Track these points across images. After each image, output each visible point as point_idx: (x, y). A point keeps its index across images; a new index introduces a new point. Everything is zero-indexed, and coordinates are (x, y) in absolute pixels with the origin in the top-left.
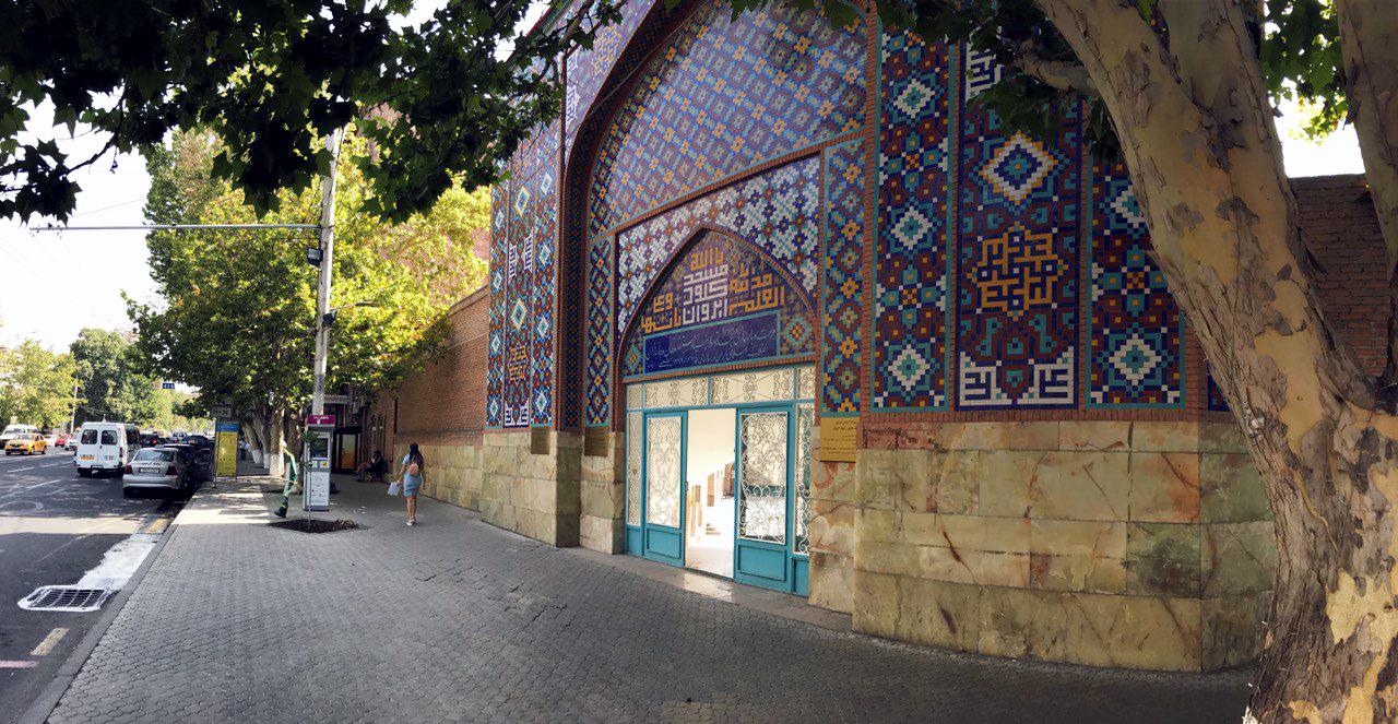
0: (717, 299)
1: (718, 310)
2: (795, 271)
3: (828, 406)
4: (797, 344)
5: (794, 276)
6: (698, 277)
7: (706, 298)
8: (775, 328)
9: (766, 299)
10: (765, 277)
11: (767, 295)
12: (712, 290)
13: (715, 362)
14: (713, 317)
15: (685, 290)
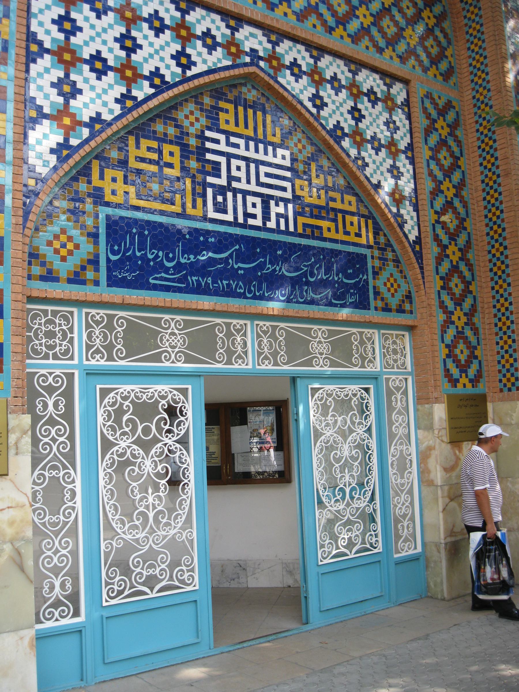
1: (278, 215)
4: (394, 303)
6: (237, 146)
7: (253, 187)
12: (263, 179)
14: (271, 224)
15: (209, 156)
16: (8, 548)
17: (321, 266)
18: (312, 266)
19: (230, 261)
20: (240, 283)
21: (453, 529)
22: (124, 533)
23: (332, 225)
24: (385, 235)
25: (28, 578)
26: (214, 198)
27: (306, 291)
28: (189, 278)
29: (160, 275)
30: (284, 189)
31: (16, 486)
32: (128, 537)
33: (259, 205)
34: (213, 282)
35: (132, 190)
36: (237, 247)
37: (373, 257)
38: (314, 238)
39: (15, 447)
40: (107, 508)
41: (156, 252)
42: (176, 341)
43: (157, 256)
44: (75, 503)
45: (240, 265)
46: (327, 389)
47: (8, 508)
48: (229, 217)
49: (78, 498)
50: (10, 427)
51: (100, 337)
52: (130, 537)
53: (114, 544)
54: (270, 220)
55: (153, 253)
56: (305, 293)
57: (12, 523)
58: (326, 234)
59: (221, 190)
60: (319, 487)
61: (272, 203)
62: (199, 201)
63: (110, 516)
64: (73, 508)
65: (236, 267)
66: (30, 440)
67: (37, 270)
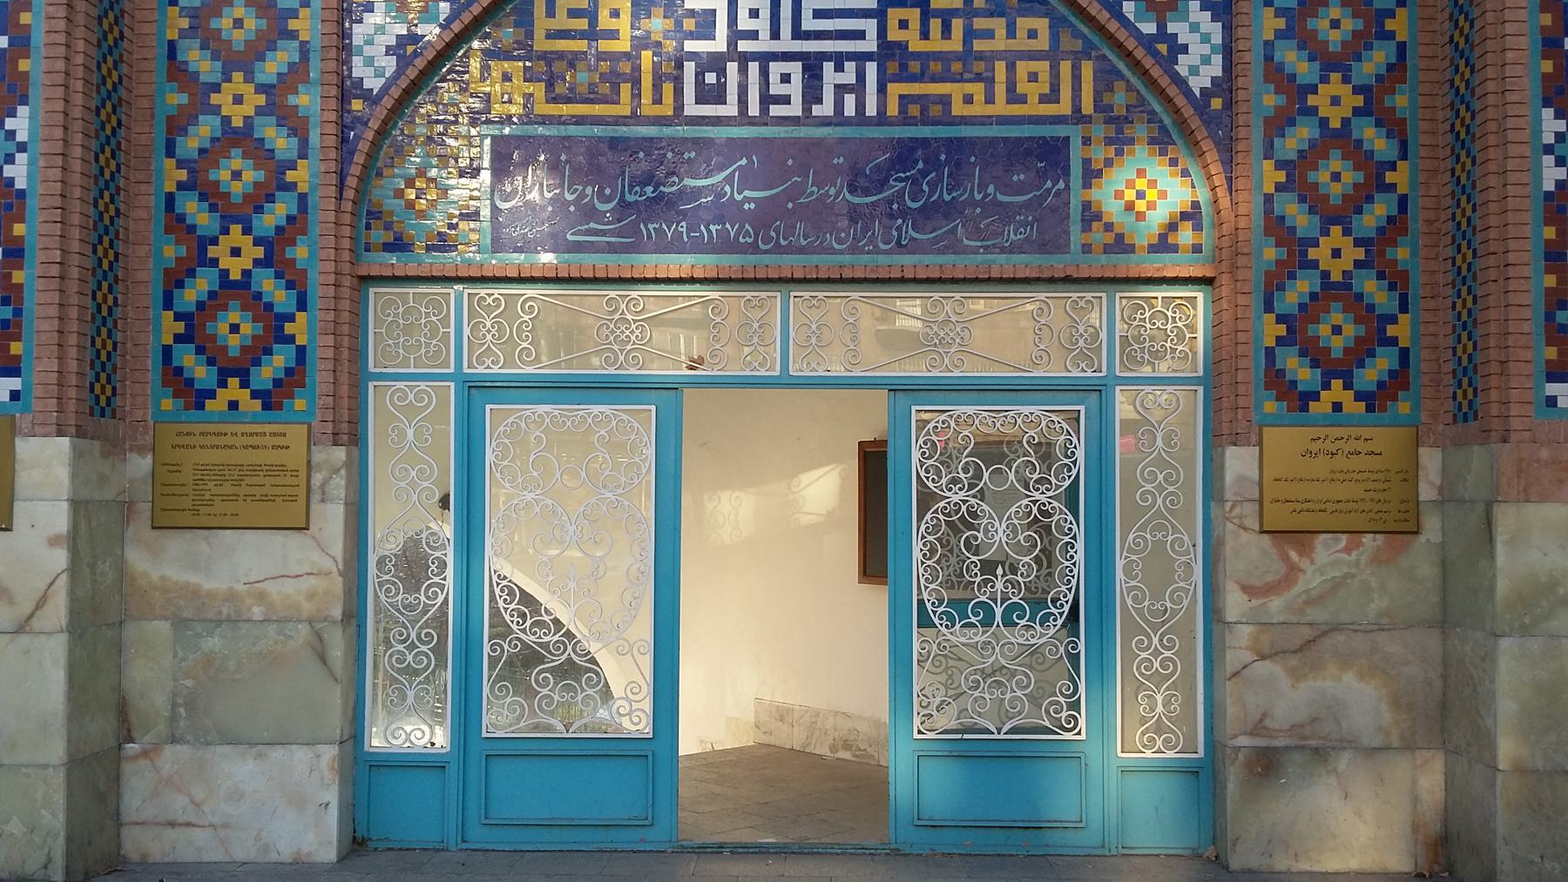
0: (839, 60)
1: (841, 89)
2: (1149, 28)
3: (1395, 398)
5: (1148, 42)
7: (787, 44)
8: (1066, 172)
9: (1032, 91)
10: (1024, 24)
11: (1033, 77)
12: (808, 24)
13: (831, 251)
14: (826, 109)
16: (304, 629)
17: (940, 179)
18: (915, 182)
19: (727, 189)
20: (747, 226)
21: (1261, 721)
22: (524, 631)
23: (977, 89)
24: (1130, 88)
25: (331, 673)
26: (700, 75)
27: (899, 229)
28: (642, 226)
29: (586, 227)
30: (860, 35)
31: (319, 545)
32: (530, 639)
33: (797, 79)
34: (689, 231)
35: (538, 90)
36: (744, 162)
37: (1087, 141)
38: (925, 120)
39: (320, 491)
40: (497, 591)
41: (581, 188)
42: (627, 332)
43: (583, 195)
44: (444, 579)
45: (747, 193)
46: (957, 413)
47: (307, 574)
48: (730, 109)
49: (450, 572)
50: (313, 464)
51: (494, 331)
52: (533, 638)
53: (506, 647)
54: (819, 101)
55: (577, 190)
56: (895, 233)
57: (311, 596)
58: (958, 109)
59: (716, 63)
60: (925, 596)
61: (828, 67)
62: (668, 88)
63: (501, 603)
64: (442, 587)
65: (738, 197)
66: (343, 483)
67: (379, 235)
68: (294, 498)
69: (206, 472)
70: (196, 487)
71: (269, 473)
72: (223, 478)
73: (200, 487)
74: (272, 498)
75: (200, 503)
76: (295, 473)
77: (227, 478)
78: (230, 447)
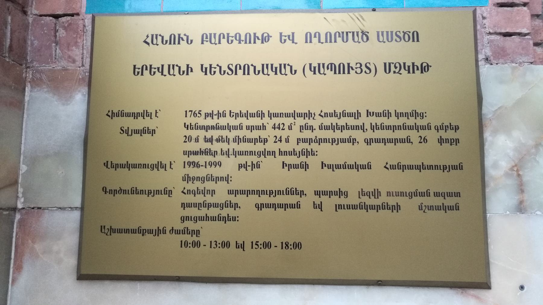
39: (511, 182)
68: (450, 201)
69: (216, 134)
70: (193, 172)
71: (379, 134)
72: (259, 147)
73: (202, 172)
74: (392, 201)
75: (203, 212)
76: (450, 134)
77: (270, 146)
78: (278, 70)
